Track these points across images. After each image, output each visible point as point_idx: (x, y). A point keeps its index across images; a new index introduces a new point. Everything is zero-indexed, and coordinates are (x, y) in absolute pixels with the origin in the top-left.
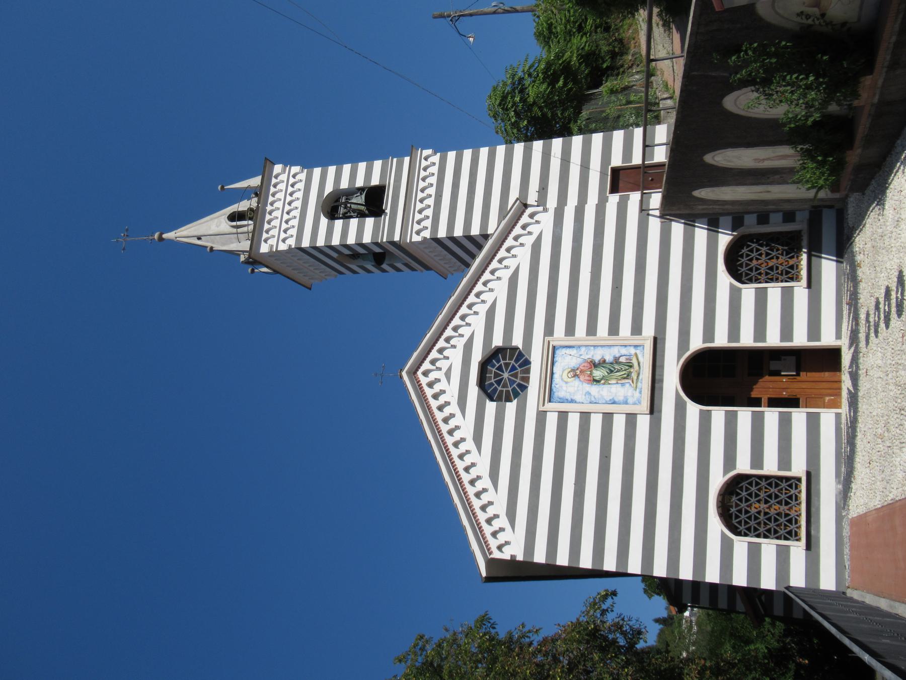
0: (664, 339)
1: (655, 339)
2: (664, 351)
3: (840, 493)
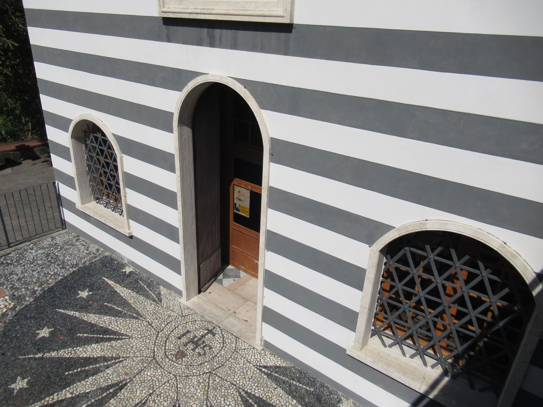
0: (286, 51)
1: (287, 28)
2: (263, 49)
3: (122, 258)
